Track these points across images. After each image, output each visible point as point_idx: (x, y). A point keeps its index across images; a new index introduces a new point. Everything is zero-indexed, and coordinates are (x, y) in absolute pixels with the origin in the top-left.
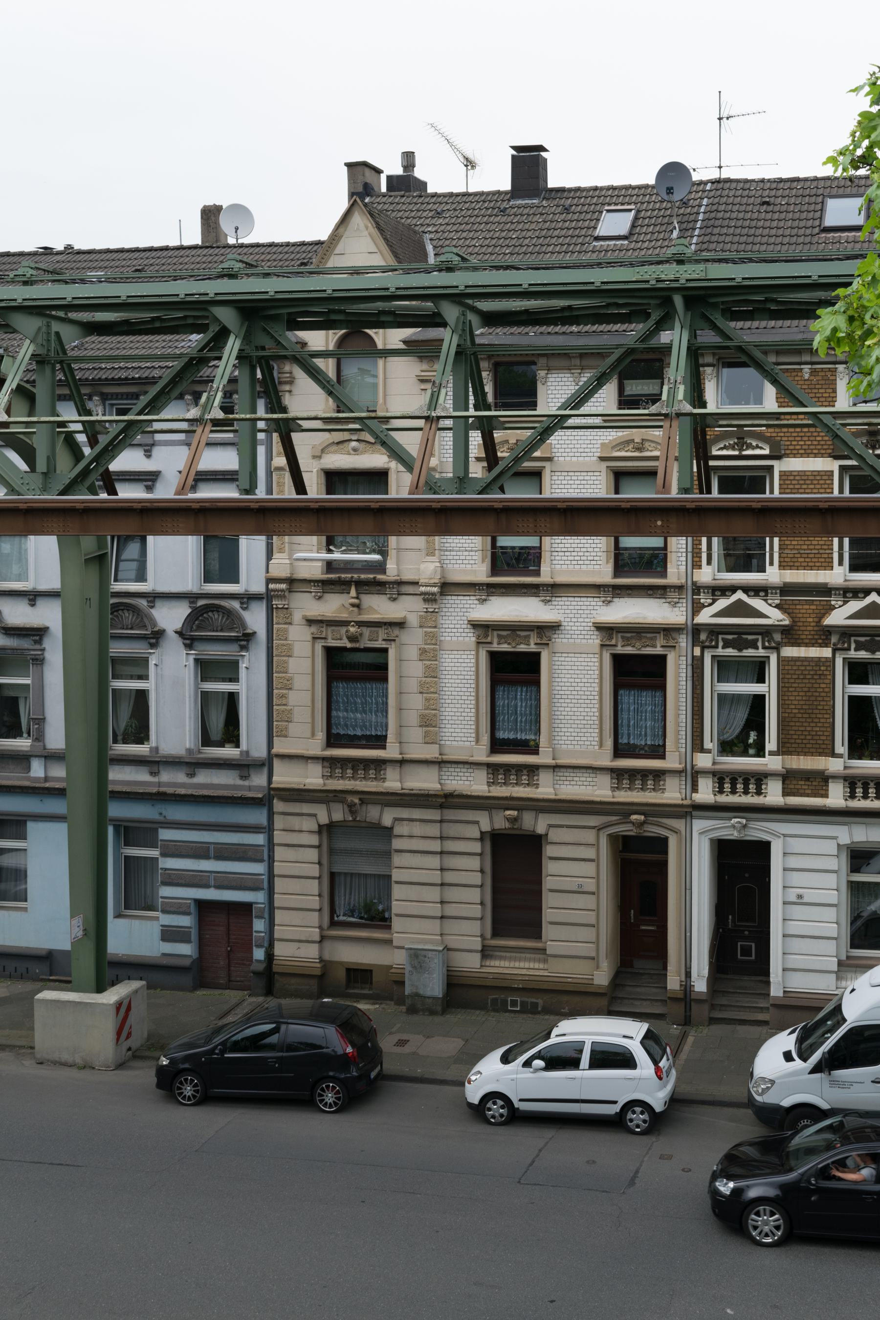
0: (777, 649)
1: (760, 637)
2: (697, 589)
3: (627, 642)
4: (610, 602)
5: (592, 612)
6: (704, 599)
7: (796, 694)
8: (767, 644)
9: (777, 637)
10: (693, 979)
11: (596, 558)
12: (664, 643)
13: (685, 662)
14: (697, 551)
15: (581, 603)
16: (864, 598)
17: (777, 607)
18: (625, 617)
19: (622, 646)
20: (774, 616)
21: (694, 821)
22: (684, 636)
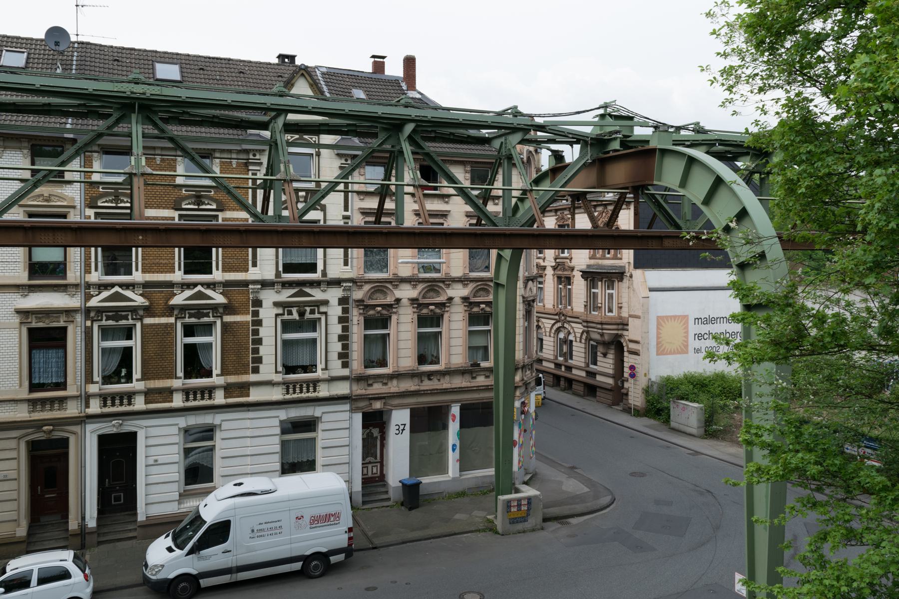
0: (141, 319)
1: (130, 313)
2: (88, 286)
3: (39, 320)
4: (26, 295)
5: (13, 302)
6: (93, 292)
7: (153, 345)
8: (134, 317)
9: (141, 312)
10: (86, 521)
11: (15, 268)
12: (65, 319)
13: (80, 330)
14: (88, 263)
15: (5, 297)
16: (194, 288)
17: (141, 295)
18: (38, 305)
19: (36, 323)
20: (139, 300)
21: (87, 425)
22: (80, 315)
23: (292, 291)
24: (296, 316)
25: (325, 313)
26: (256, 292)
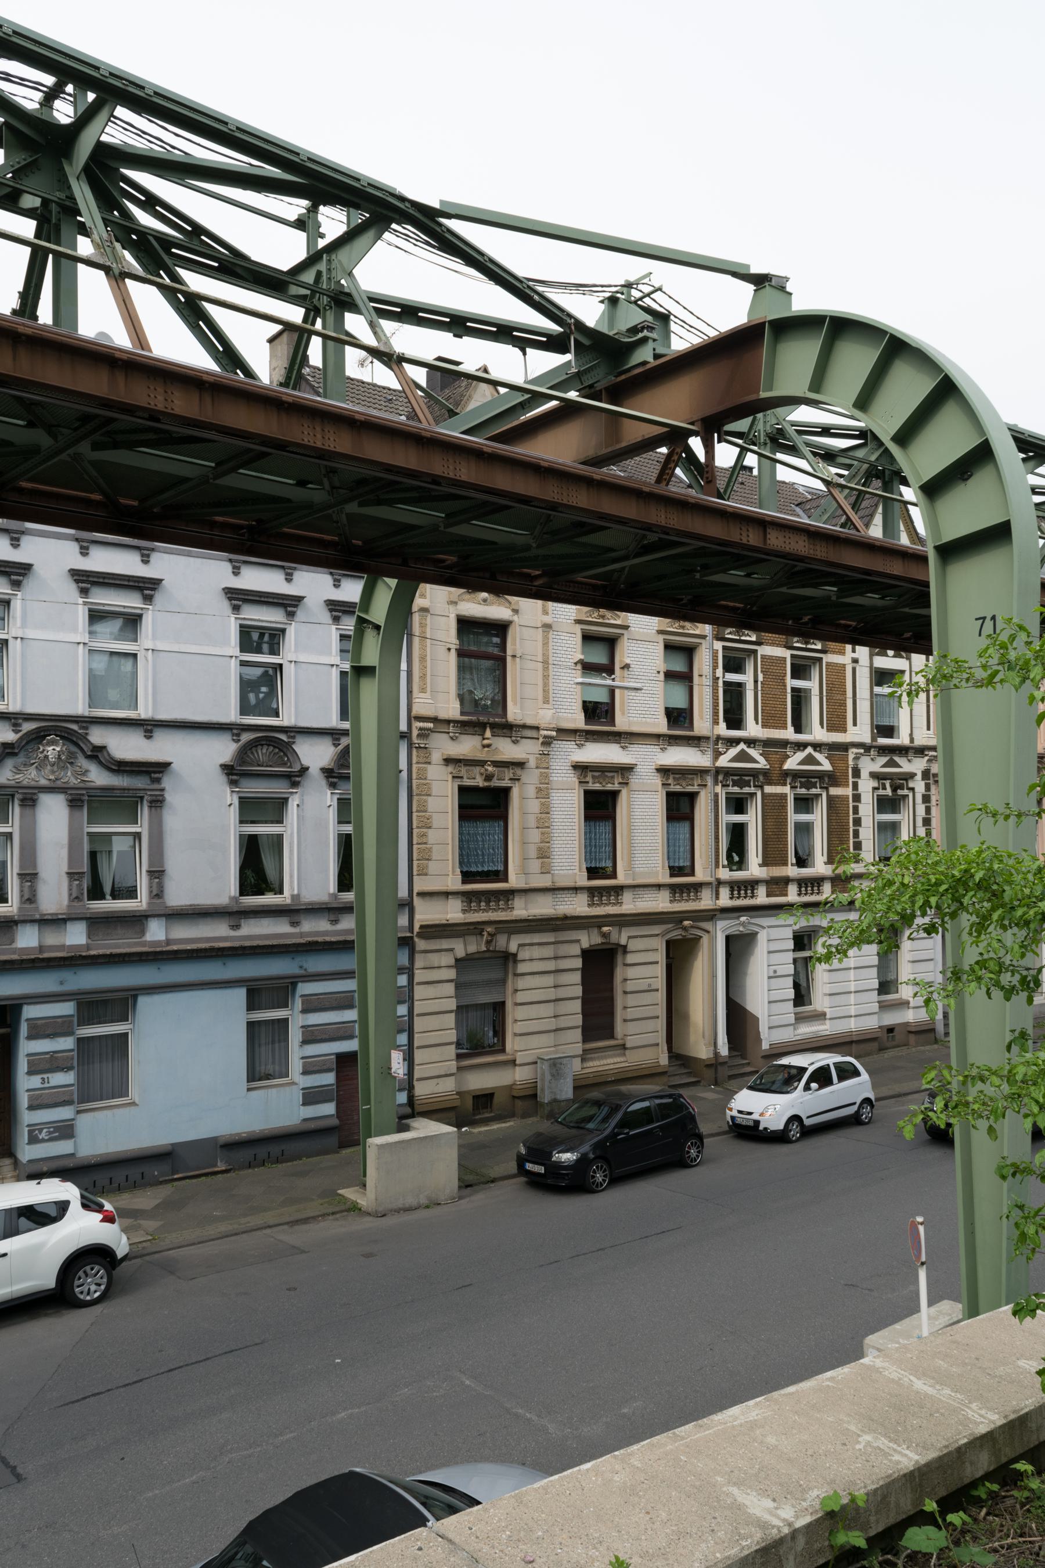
0: (761, 787)
1: (752, 778)
2: (719, 738)
9: (761, 778)
12: (699, 782)
16: (803, 750)
17: (761, 755)
20: (762, 763)
22: (709, 777)
23: (884, 760)
24: (889, 792)
25: (913, 789)
26: (857, 758)
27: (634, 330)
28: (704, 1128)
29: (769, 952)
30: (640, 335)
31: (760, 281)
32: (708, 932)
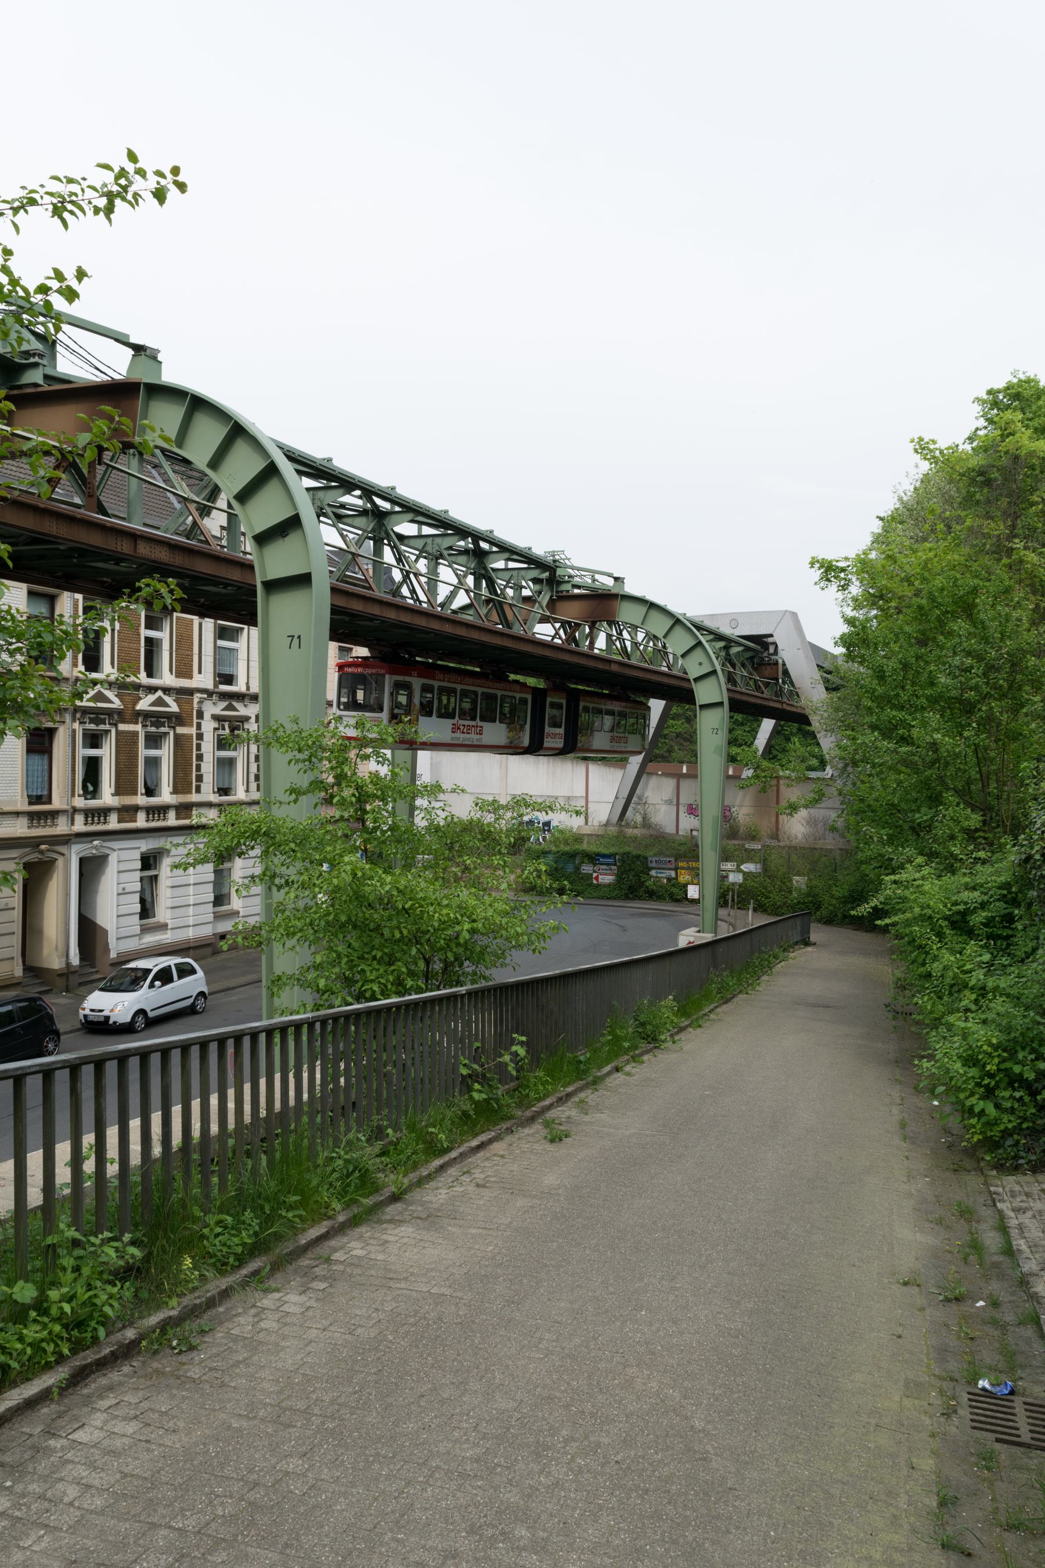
0: (116, 725)
9: (116, 717)
20: (117, 704)
23: (224, 704)
27: (27, 354)
28: (61, 1026)
29: (119, 872)
30: (32, 360)
31: (138, 349)
32: (63, 855)
